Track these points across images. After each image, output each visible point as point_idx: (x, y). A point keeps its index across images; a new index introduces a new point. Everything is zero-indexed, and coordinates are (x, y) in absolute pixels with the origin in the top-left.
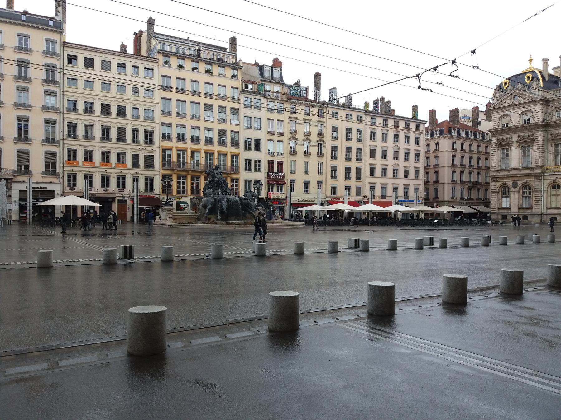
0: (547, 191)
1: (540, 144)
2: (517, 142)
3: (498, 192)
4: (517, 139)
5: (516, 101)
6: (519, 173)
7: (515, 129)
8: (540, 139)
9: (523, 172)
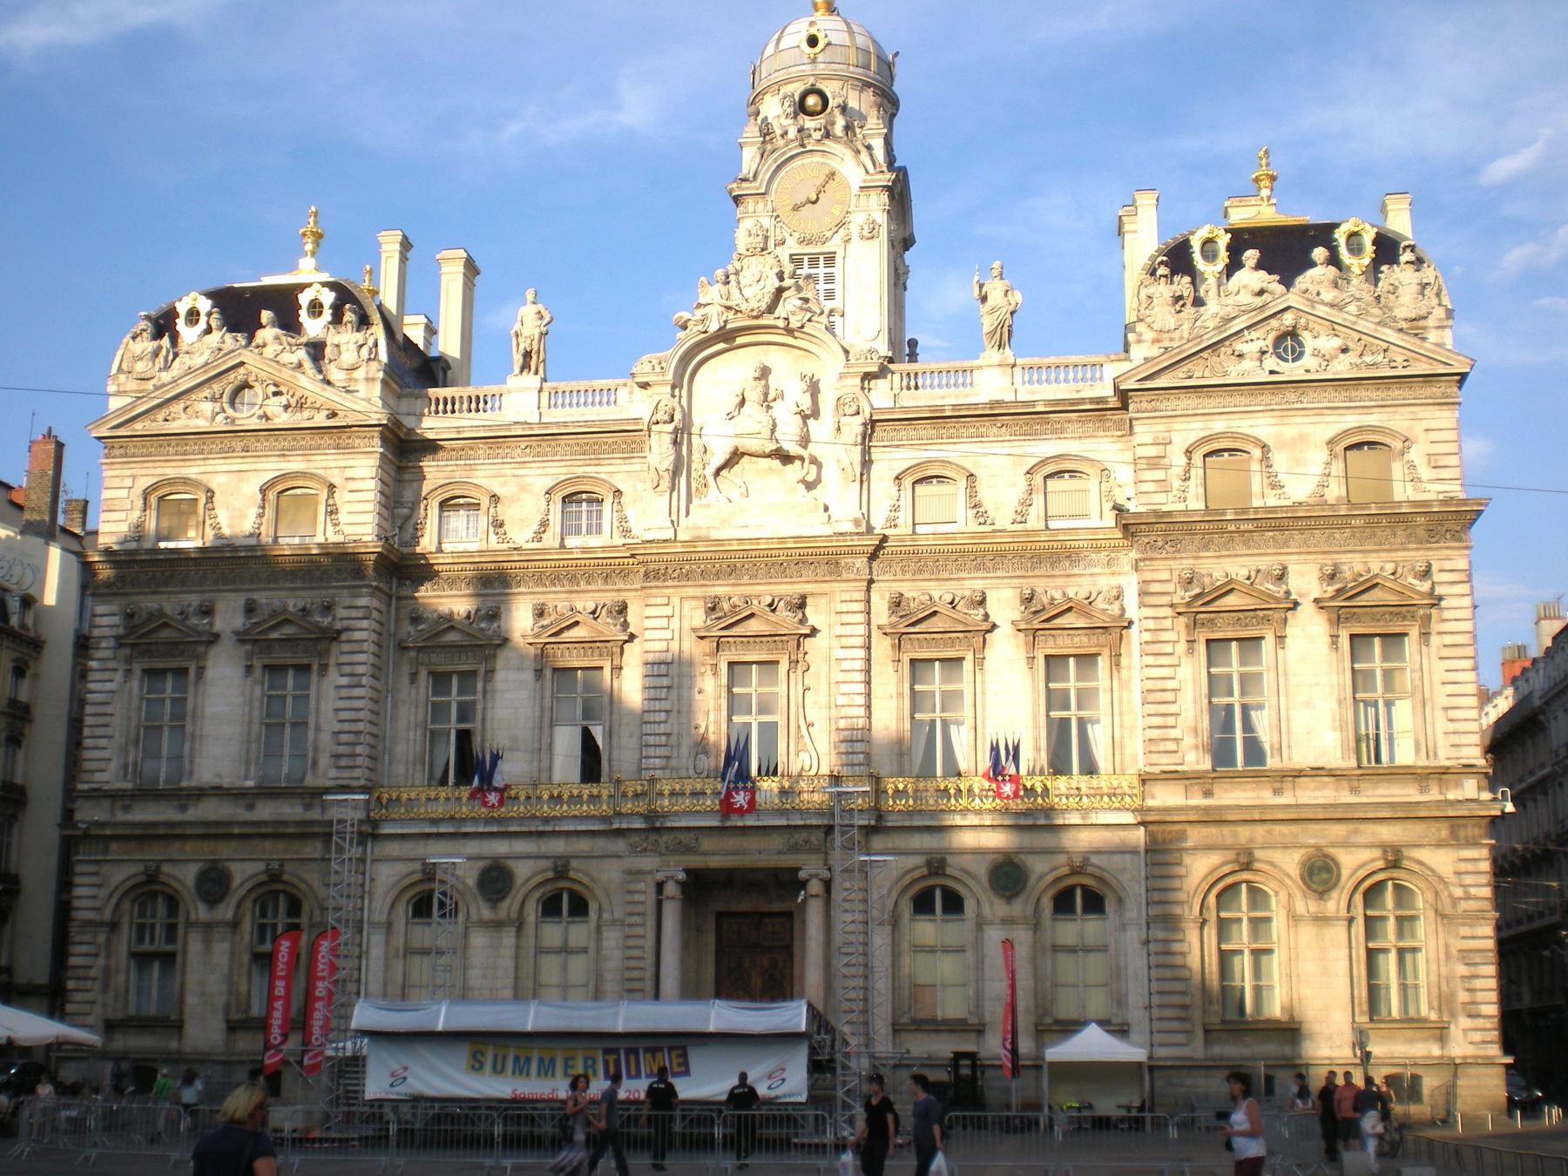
0: (389, 926)
1: (364, 660)
2: (242, 637)
3: (113, 926)
4: (239, 622)
5: (247, 418)
6: (242, 814)
8: (364, 632)
9: (265, 811)
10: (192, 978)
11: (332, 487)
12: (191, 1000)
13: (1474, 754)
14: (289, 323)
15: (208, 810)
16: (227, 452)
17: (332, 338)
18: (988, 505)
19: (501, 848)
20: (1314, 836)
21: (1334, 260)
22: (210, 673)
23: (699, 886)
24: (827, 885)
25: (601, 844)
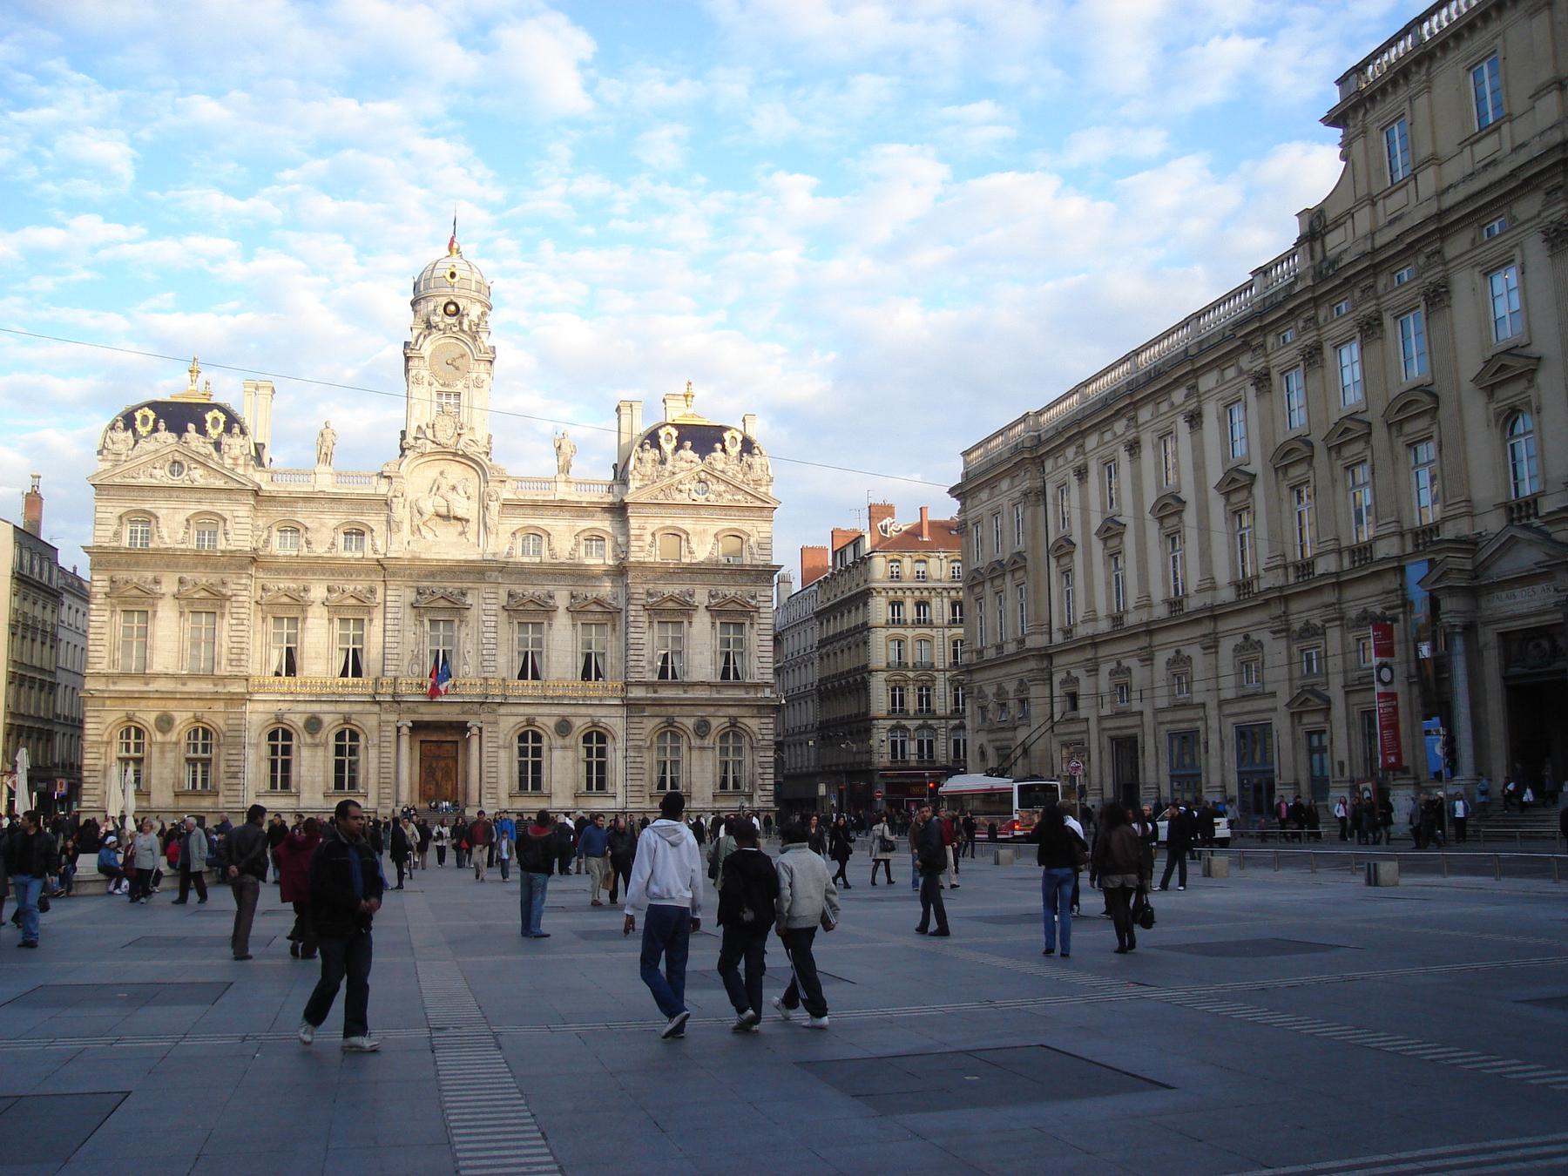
3: (109, 743)
5: (177, 481)
6: (180, 688)
7: (170, 559)
9: (192, 687)
10: (154, 771)
11: (225, 520)
12: (154, 781)
13: (769, 678)
14: (201, 430)
15: (168, 686)
17: (226, 439)
18: (557, 550)
19: (316, 708)
20: (700, 712)
21: (724, 450)
22: (159, 614)
23: (417, 727)
24: (480, 729)
25: (368, 707)
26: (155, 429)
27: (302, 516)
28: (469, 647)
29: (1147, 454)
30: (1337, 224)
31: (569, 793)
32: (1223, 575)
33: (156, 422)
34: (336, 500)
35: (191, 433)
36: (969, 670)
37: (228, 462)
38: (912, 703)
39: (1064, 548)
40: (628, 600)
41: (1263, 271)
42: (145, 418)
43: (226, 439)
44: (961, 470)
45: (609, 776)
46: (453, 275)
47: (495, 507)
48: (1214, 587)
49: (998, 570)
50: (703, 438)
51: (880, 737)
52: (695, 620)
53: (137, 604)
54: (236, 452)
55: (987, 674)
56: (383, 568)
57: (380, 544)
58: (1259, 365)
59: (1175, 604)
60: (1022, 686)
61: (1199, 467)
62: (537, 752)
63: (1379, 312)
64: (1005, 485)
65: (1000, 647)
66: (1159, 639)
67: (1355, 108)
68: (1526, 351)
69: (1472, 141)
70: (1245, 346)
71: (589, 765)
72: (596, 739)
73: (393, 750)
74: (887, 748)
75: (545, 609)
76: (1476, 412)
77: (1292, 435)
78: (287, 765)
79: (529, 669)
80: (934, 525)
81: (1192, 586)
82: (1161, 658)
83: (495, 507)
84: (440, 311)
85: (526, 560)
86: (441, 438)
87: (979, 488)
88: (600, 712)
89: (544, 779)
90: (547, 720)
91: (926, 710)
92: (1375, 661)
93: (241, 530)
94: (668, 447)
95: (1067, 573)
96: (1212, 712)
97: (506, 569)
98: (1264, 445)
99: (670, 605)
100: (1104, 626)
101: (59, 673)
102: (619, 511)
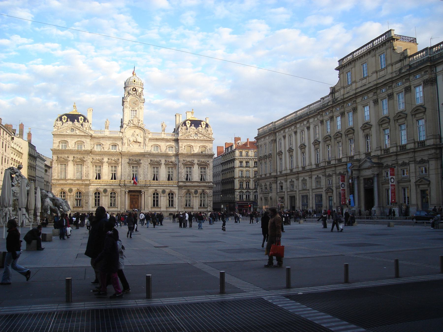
5: (72, 133)
7: (71, 152)
8: (89, 161)
9: (77, 182)
14: (78, 121)
15: (71, 182)
16: (70, 137)
17: (84, 123)
19: (106, 187)
23: (130, 192)
25: (118, 187)
26: (67, 121)
27: (102, 141)
28: (141, 173)
29: (298, 134)
30: (337, 91)
31: (165, 207)
32: (313, 162)
33: (67, 119)
34: (110, 138)
35: (76, 122)
36: (259, 179)
37: (85, 129)
38: (244, 186)
39: (280, 153)
40: (179, 162)
41: (323, 98)
42: (65, 118)
43: (84, 123)
44: (257, 133)
45: (174, 203)
46: (134, 81)
47: (147, 140)
48: (311, 165)
49: (265, 157)
50: (196, 123)
51: (237, 193)
52: (195, 167)
53: (64, 163)
54: (86, 126)
55: (263, 181)
56: (121, 154)
57: (120, 148)
58: (321, 119)
59: (303, 168)
60: (271, 184)
61: (309, 138)
62: (157, 197)
63: (344, 111)
64: (267, 138)
65: (266, 175)
66: (300, 175)
67: (341, 68)
68: (370, 123)
69: (362, 79)
70: (319, 114)
71: (169, 201)
72: (171, 194)
73: (124, 197)
74: (238, 197)
75: (159, 164)
76: (361, 134)
77: (327, 134)
78: (99, 200)
79: (155, 178)
80: (250, 142)
81: (307, 164)
82: (301, 179)
83: (147, 140)
84: (132, 90)
85: (154, 152)
86: (135, 123)
87: (262, 138)
88: (172, 188)
89: (159, 204)
90: (160, 190)
91: (248, 188)
92: (341, 183)
93: (88, 145)
94: (188, 126)
95: (281, 159)
96: (311, 191)
97: (150, 154)
98: (322, 136)
99: (189, 163)
100: (289, 171)
101: (36, 177)
102: (177, 141)
